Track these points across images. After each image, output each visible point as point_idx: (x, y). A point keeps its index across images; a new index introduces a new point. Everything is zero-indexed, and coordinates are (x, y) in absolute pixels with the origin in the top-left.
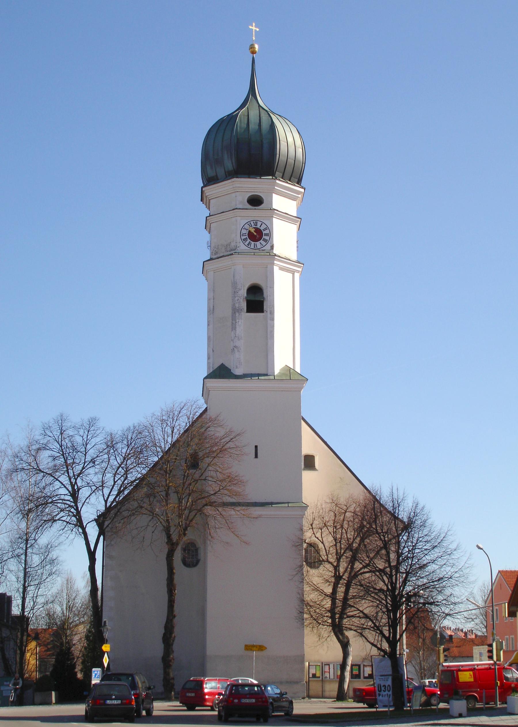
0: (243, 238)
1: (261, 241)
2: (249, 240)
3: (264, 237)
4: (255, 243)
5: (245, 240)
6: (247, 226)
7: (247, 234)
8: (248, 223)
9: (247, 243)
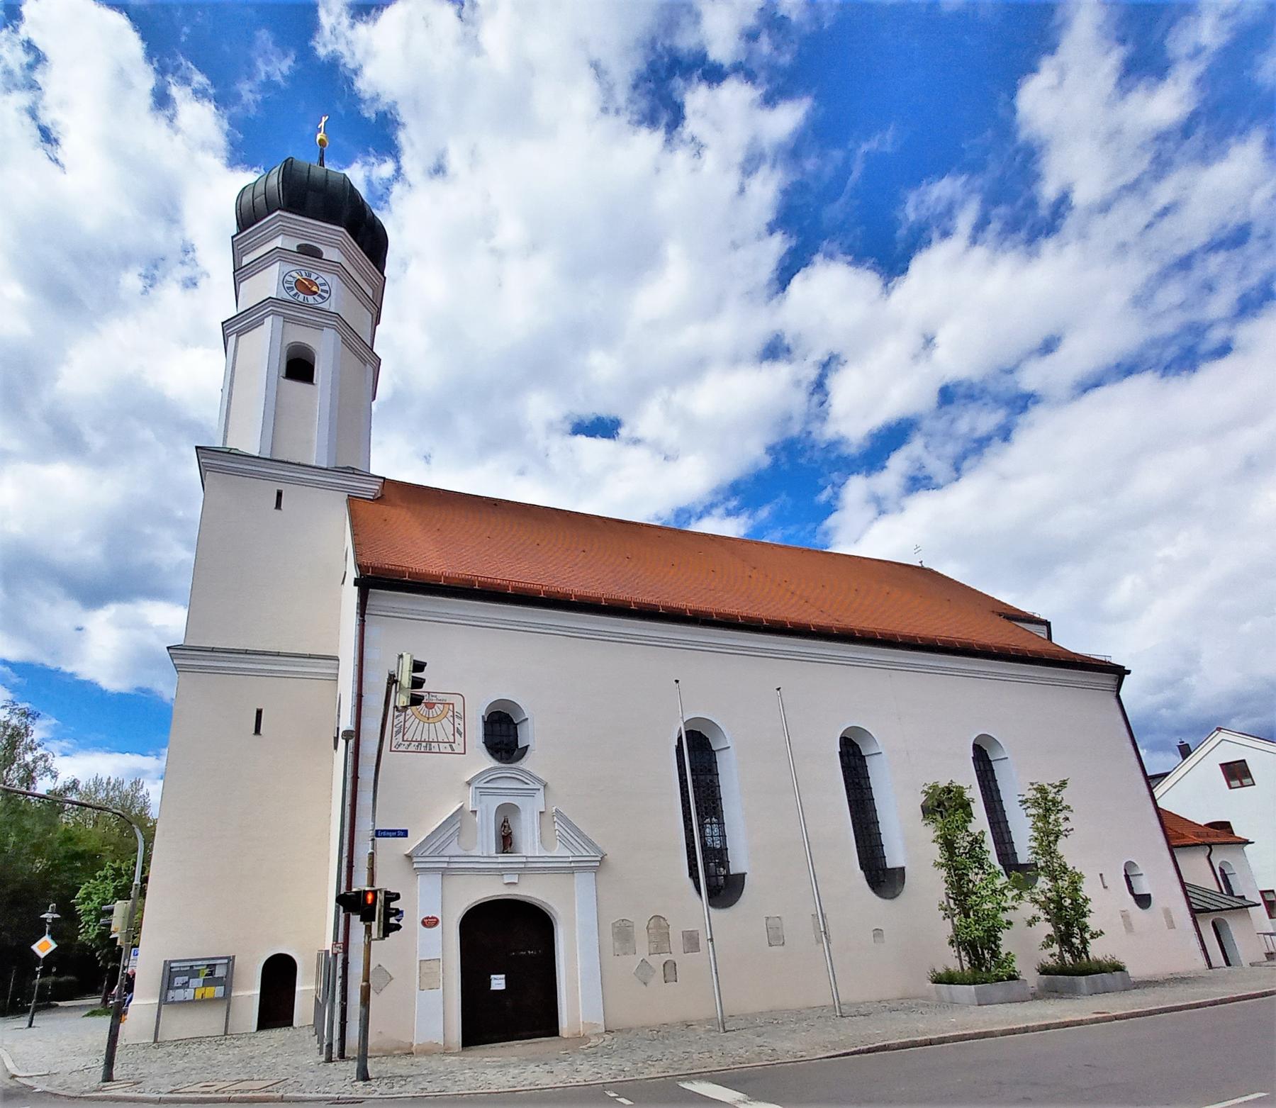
0: (286, 285)
2: (295, 291)
4: (306, 296)
5: (291, 289)
6: (294, 274)
7: (294, 283)
9: (292, 293)
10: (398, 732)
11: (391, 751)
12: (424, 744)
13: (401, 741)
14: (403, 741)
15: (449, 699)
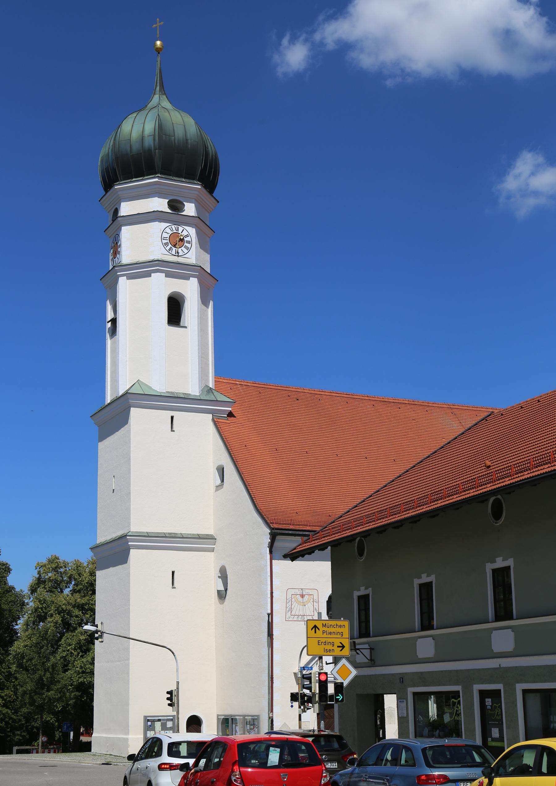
0: (164, 241)
1: (183, 248)
2: (170, 246)
3: (185, 244)
6: (168, 230)
7: (168, 238)
8: (169, 227)
9: (168, 248)
10: (288, 611)
11: (286, 621)
12: (300, 617)
13: (290, 616)
14: (291, 615)
15: (311, 592)
